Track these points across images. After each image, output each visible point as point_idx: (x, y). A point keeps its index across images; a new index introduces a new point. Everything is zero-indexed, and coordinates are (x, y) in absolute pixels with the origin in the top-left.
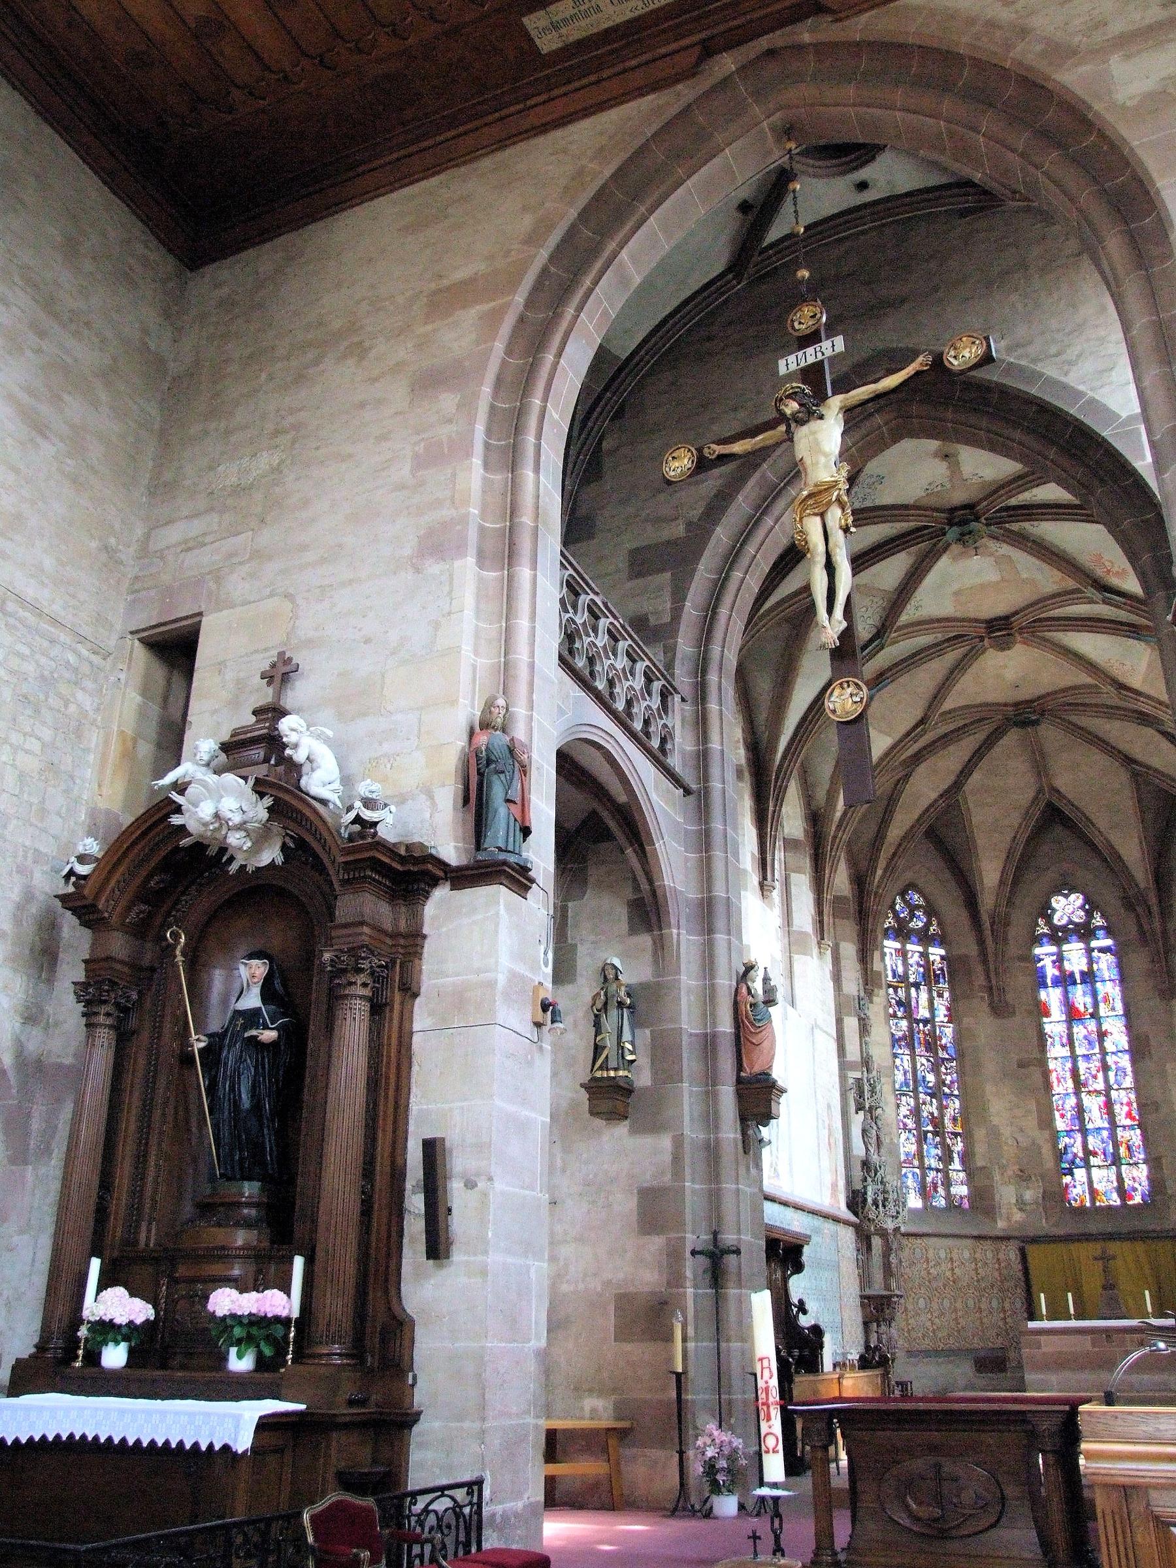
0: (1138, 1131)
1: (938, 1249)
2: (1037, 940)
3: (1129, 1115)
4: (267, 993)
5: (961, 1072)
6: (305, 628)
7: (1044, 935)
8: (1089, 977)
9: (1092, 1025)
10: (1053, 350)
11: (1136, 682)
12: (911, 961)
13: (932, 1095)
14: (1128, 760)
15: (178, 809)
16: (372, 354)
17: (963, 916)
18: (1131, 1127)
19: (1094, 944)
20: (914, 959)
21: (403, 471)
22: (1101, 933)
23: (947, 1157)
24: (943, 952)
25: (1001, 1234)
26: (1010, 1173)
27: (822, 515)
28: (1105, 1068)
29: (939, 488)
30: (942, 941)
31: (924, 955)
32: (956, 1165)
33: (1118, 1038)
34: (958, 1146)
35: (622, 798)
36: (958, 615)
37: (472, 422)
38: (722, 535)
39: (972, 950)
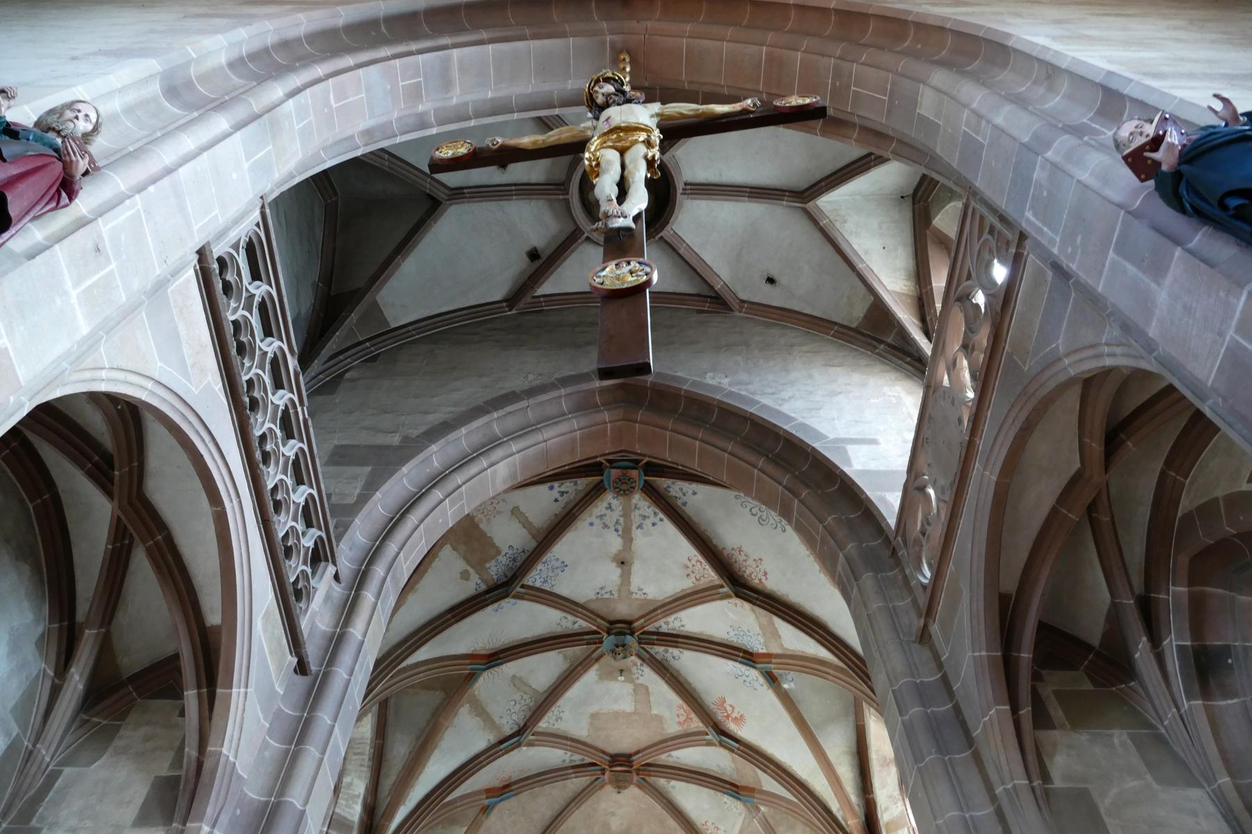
10: (770, 390)
29: (607, 596)
35: (214, 617)
36: (588, 740)
38: (436, 455)
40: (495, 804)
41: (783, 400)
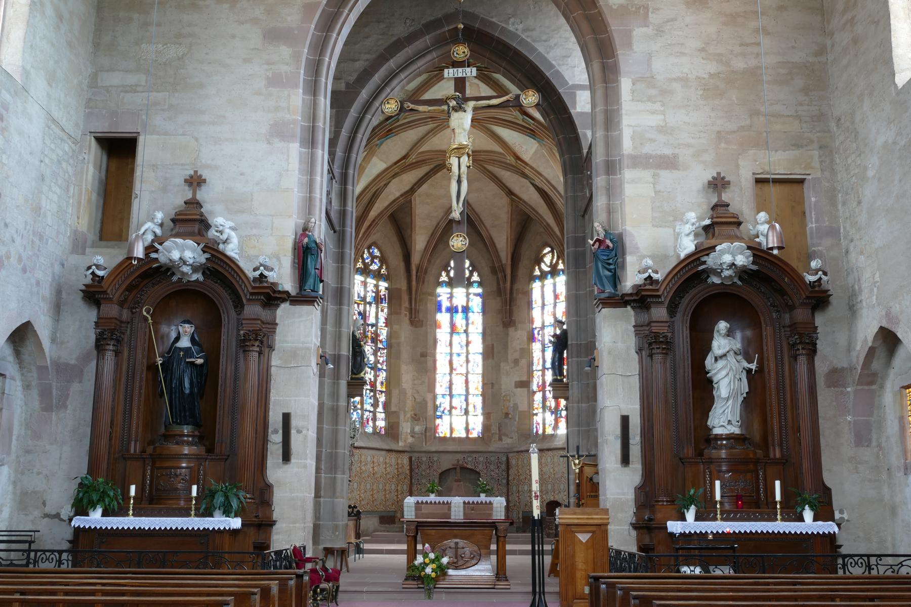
0: (481, 398)
1: (368, 456)
2: (440, 284)
3: (477, 388)
4: (193, 340)
5: (389, 355)
7: (444, 281)
8: (466, 310)
9: (464, 336)
10: (544, 38)
11: (526, 157)
12: (368, 289)
13: (372, 368)
14: (510, 193)
15: (157, 251)
17: (402, 265)
18: (477, 395)
19: (472, 290)
20: (371, 287)
22: (476, 285)
23: (375, 405)
24: (386, 285)
25: (400, 449)
26: (409, 415)
27: (459, 158)
28: (468, 361)
30: (386, 278)
31: (377, 286)
32: (380, 409)
33: (477, 345)
34: (382, 398)
38: (364, 94)
39: (403, 285)
40: (382, 143)
41: (550, 47)
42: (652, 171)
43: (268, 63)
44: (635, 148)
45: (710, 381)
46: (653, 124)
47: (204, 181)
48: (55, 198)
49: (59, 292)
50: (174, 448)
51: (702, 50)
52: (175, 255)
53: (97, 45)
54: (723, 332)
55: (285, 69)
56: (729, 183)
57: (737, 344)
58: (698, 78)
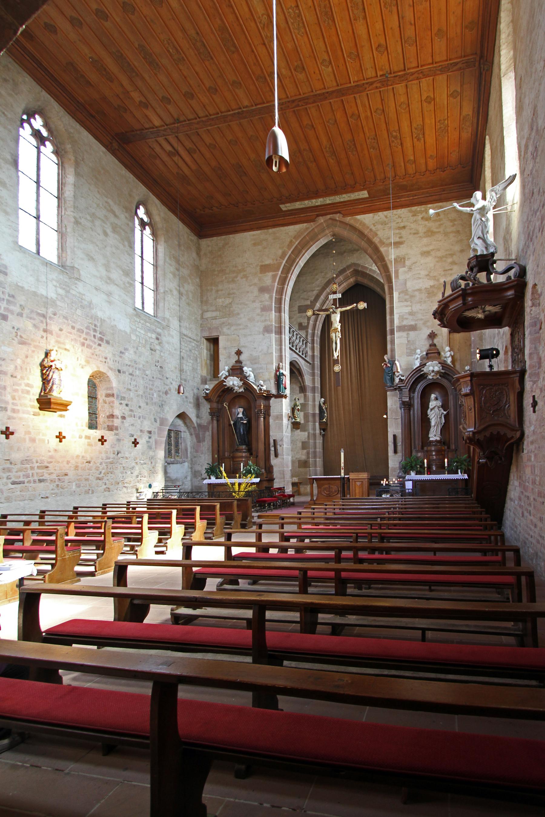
6: (242, 343)
16: (249, 278)
21: (258, 311)
37: (272, 303)
42: (406, 333)
43: (261, 302)
44: (400, 323)
45: (429, 419)
46: (407, 311)
47: (242, 353)
48: (191, 364)
49: (197, 399)
50: (240, 454)
51: (428, 275)
52: (231, 383)
53: (202, 302)
54: (433, 399)
55: (267, 303)
56: (436, 335)
57: (439, 403)
58: (426, 288)
